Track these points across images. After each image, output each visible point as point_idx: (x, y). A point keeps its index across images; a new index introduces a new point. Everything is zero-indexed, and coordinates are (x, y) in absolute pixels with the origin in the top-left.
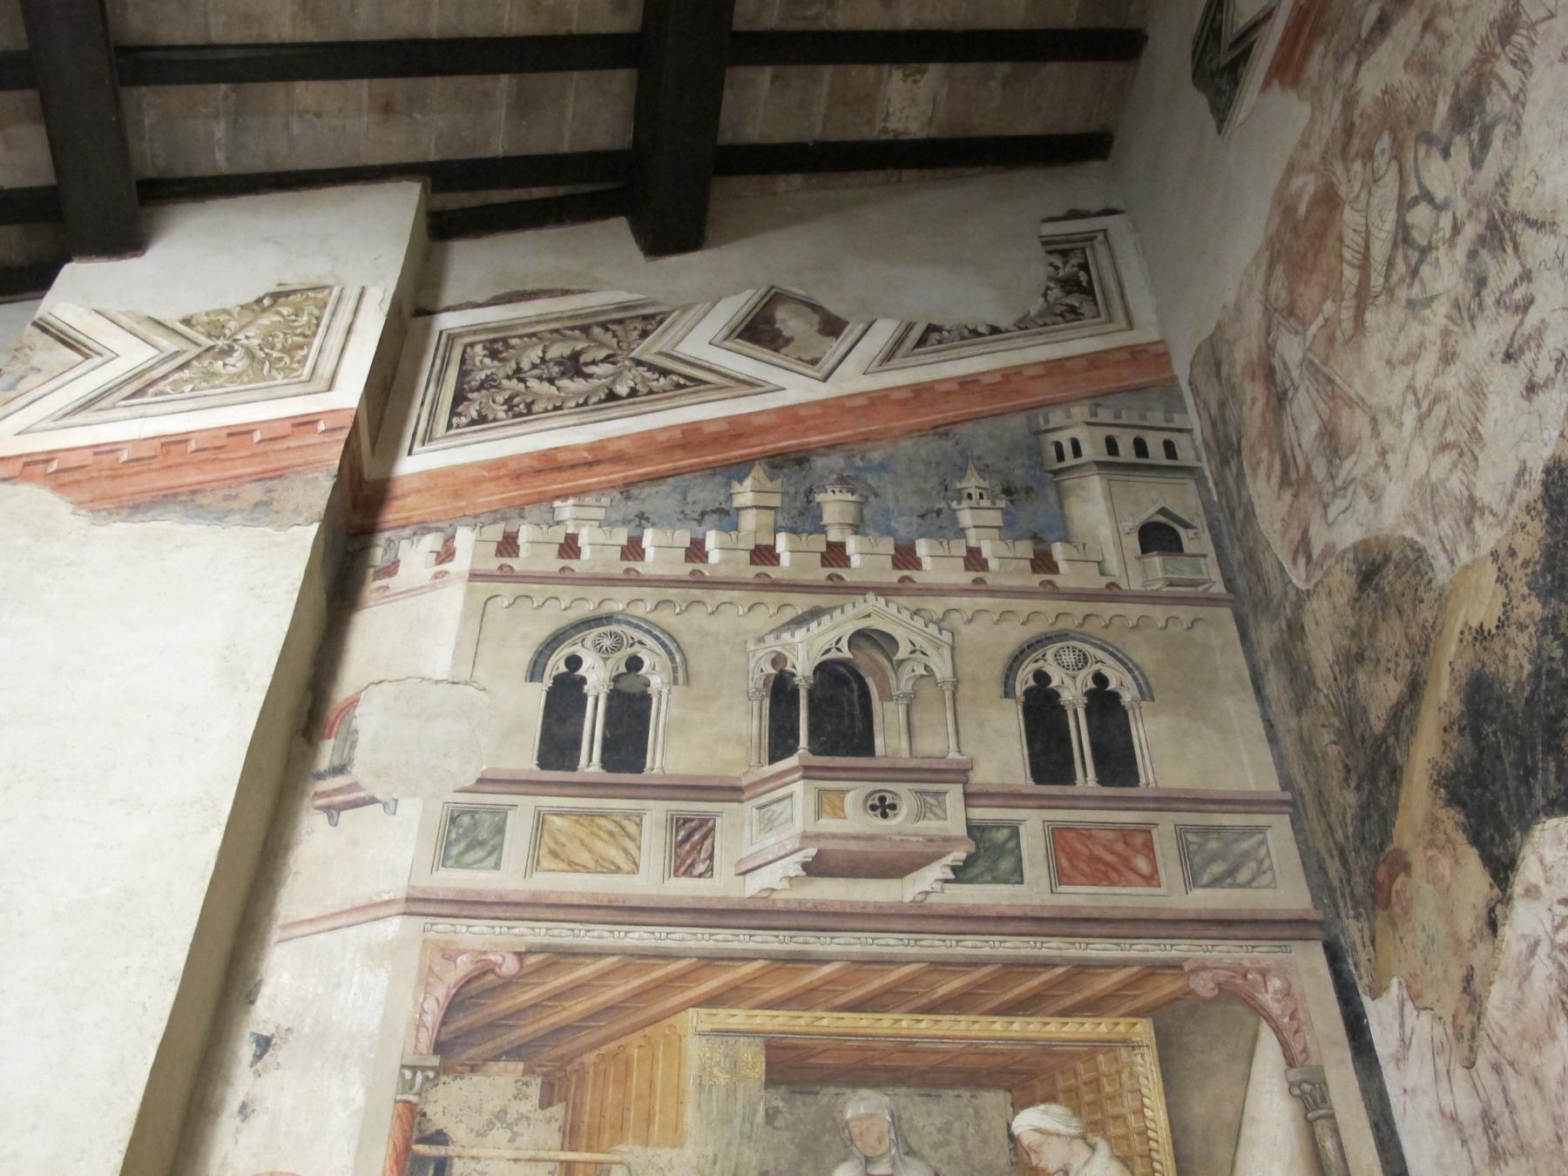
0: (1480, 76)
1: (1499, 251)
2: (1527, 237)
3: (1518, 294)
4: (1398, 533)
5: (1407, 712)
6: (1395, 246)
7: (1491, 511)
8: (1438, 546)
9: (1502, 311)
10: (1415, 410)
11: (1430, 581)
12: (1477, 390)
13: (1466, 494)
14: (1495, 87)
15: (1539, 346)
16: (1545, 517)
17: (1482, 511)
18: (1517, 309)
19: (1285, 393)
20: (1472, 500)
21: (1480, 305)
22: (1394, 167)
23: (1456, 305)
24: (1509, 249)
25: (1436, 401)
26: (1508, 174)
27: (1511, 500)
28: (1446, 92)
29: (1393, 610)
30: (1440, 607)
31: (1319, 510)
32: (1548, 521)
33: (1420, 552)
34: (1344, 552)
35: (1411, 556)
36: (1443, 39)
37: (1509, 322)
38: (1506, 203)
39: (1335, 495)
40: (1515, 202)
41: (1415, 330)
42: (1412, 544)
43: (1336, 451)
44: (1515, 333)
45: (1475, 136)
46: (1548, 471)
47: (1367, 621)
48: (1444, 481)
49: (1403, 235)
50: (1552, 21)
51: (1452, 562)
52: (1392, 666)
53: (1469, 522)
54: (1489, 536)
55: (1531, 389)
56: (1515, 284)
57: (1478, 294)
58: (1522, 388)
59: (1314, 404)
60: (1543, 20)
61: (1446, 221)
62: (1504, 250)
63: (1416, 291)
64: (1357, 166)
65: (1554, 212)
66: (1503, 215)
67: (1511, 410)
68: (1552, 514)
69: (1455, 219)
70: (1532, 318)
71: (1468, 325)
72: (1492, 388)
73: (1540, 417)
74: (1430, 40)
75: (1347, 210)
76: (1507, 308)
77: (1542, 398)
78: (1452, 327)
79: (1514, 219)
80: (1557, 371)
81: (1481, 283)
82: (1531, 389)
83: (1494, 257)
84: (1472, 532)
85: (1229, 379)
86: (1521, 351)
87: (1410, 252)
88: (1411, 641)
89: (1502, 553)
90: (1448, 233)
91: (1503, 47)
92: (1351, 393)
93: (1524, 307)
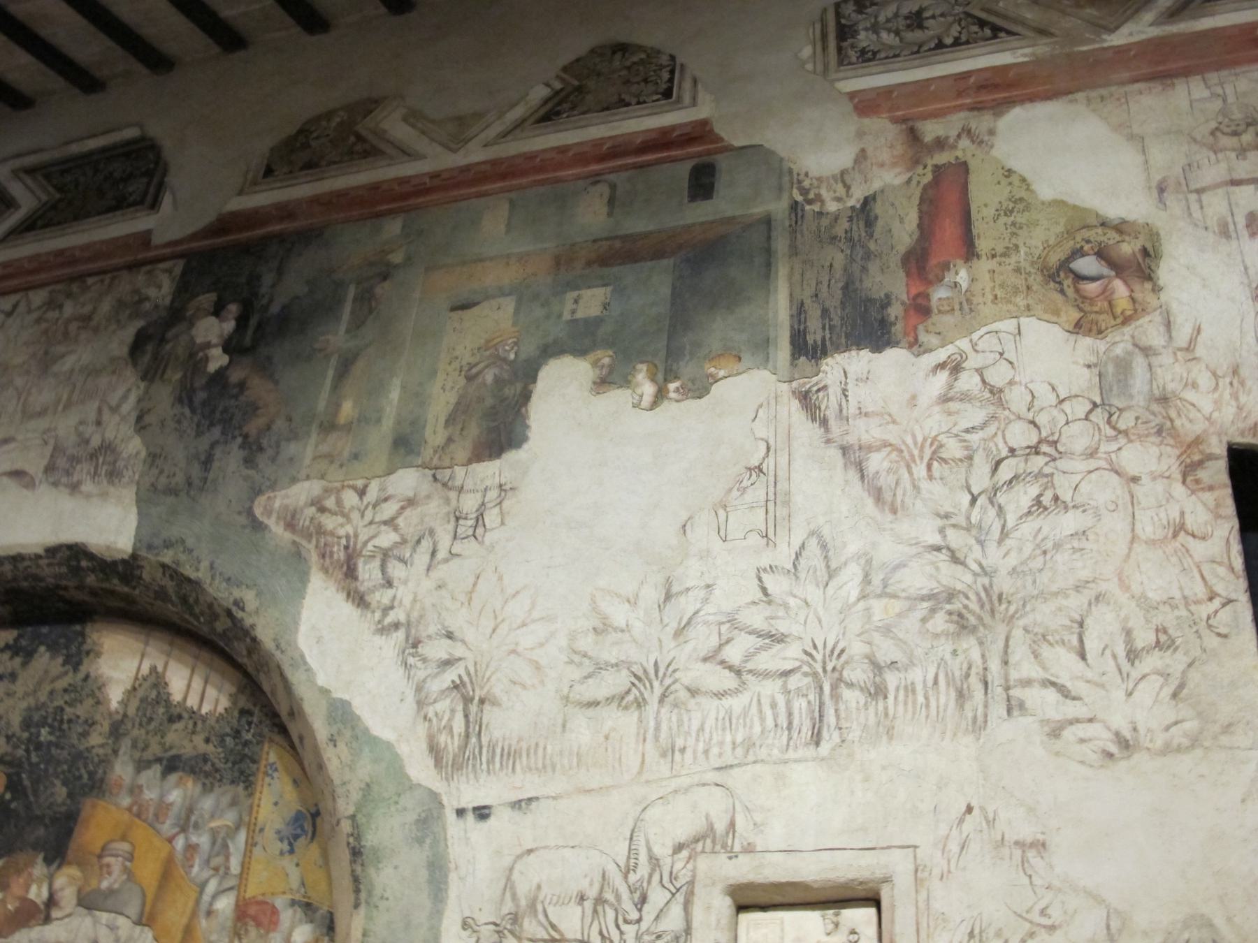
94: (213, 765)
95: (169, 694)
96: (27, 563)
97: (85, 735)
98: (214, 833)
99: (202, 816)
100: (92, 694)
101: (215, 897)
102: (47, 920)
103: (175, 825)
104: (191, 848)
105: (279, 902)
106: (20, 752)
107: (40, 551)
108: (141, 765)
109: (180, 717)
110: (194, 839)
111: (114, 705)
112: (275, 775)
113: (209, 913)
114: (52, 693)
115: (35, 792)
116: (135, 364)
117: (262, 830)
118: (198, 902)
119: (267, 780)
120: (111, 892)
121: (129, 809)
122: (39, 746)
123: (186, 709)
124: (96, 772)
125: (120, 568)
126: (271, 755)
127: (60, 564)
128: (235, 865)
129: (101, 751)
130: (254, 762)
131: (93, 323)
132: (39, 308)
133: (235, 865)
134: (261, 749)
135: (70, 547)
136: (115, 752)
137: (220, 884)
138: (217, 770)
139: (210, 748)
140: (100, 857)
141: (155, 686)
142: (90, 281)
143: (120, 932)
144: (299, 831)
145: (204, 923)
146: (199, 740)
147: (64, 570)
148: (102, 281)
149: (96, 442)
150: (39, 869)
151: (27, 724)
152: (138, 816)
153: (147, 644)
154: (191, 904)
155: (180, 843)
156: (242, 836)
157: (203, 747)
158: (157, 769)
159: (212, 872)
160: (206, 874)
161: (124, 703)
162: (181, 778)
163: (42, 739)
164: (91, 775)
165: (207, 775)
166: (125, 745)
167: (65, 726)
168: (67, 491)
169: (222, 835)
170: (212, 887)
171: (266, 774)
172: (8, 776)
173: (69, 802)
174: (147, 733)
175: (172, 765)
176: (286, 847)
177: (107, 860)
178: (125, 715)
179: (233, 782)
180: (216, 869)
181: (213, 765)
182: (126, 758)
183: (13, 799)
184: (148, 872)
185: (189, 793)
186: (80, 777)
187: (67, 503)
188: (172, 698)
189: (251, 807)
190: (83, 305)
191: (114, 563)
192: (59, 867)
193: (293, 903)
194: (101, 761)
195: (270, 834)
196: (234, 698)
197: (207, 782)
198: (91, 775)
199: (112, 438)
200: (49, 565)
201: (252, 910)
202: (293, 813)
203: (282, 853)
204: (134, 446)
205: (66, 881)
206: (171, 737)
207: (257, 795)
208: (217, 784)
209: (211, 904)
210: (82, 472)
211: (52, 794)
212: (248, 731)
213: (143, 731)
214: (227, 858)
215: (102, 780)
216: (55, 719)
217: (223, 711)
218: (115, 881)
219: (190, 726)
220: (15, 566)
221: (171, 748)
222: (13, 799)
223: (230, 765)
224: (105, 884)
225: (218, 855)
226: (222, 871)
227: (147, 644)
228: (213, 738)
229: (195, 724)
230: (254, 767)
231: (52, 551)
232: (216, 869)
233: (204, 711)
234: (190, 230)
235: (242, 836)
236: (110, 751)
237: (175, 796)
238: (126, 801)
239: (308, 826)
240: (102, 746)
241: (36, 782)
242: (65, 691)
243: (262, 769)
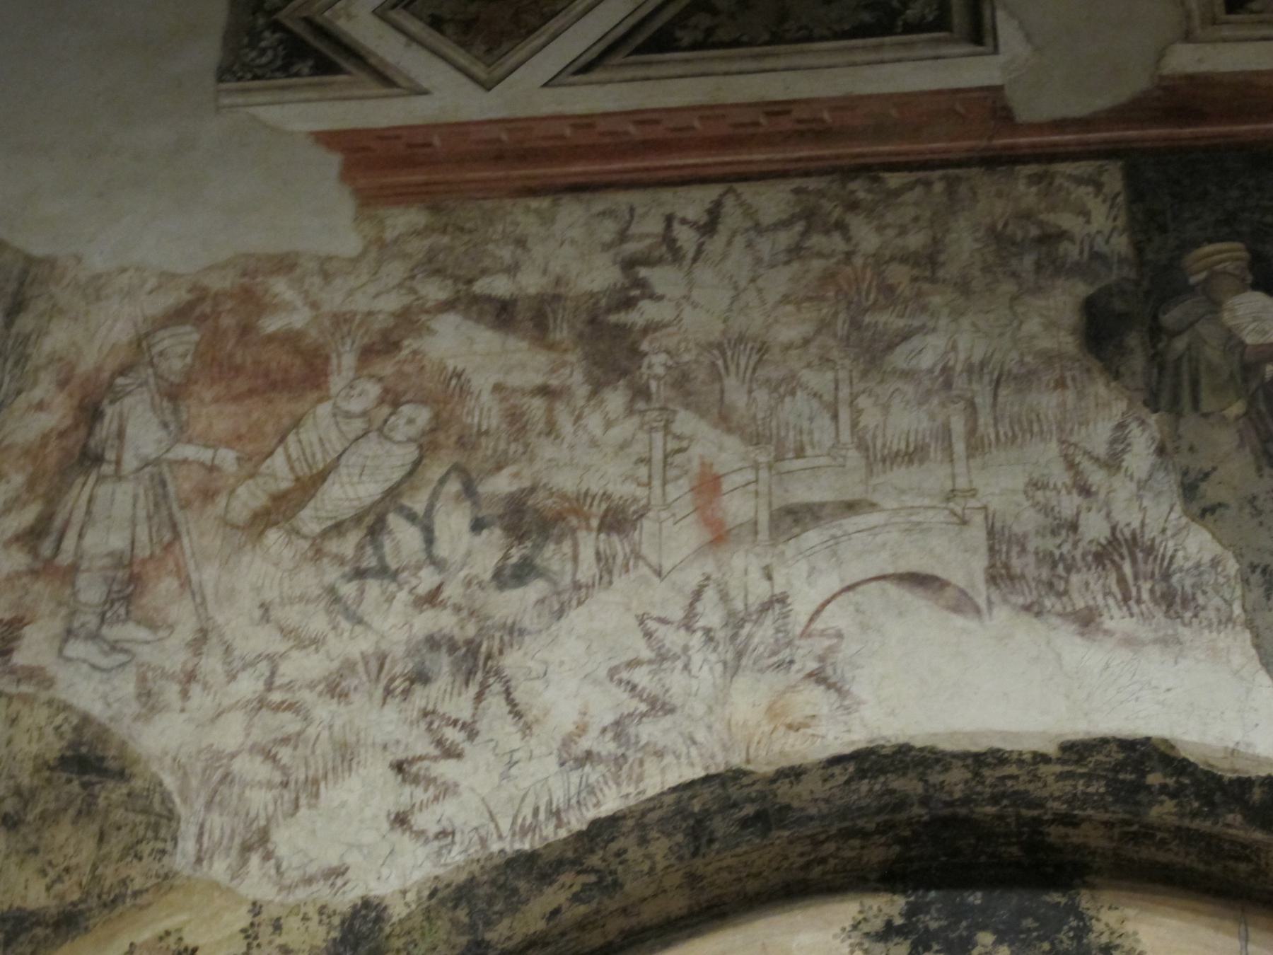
0: (560, 517)
1: (460, 679)
2: (495, 703)
3: (452, 735)
4: (154, 768)
5: (39, 932)
6: (358, 519)
7: (278, 867)
8: (194, 830)
9: (423, 725)
10: (260, 686)
11: (163, 852)
12: (346, 755)
13: (262, 823)
14: (567, 547)
15: (436, 798)
16: (335, 934)
17: (267, 856)
18: (439, 743)
19: (99, 460)
20: (264, 836)
21: (406, 693)
22: (411, 453)
23: (382, 659)
24: (473, 689)
25: (291, 707)
26: (522, 632)
27: (309, 881)
28: (516, 475)
29: (94, 828)
30: (158, 886)
31: (57, 626)
32: (334, 940)
33: (171, 816)
34: (66, 707)
35: (157, 806)
36: (551, 429)
37: (422, 746)
38: (501, 652)
39: (94, 636)
40: (511, 661)
41: (318, 623)
42: (166, 798)
43: (128, 600)
44: (421, 758)
45: (516, 555)
46: (366, 903)
47: (47, 800)
48: (245, 785)
49: (373, 523)
50: (656, 580)
51: (199, 860)
52: (52, 874)
53: (246, 849)
54: (257, 883)
55: (401, 820)
56: (455, 723)
57: (412, 682)
58: (394, 810)
59: (133, 523)
60: (650, 566)
61: (427, 580)
62: (467, 684)
63: (348, 590)
64: (374, 390)
65: (537, 721)
66: (489, 657)
67: (368, 813)
68: (343, 940)
69: (439, 589)
70: (446, 769)
71: (379, 693)
72: (362, 771)
73: (392, 852)
74: (537, 406)
75: (324, 409)
76: (429, 729)
77: (404, 841)
78: (360, 668)
79: (498, 673)
80: (437, 836)
81: (421, 677)
82: (401, 820)
83: (453, 675)
84: (244, 862)
85: (25, 340)
86: (416, 780)
87: (369, 550)
88: (95, 878)
89: (264, 916)
90: (423, 589)
91: (600, 530)
92: (194, 577)
93: (451, 753)
96: (1013, 770)
107: (1051, 749)
116: (1115, 375)
125: (1257, 794)
127: (1089, 777)
131: (950, 271)
132: (786, 224)
135: (1128, 745)
142: (894, 180)
147: (1098, 787)
148: (928, 184)
149: (1095, 528)
153: (1247, 939)
168: (1073, 627)
187: (1076, 651)
190: (903, 231)
191: (1244, 784)
199: (1136, 524)
200: (1061, 777)
204: (1198, 544)
210: (1088, 587)
220: (976, 774)
227: (1247, 939)
231: (1077, 751)
234: (1102, 102)
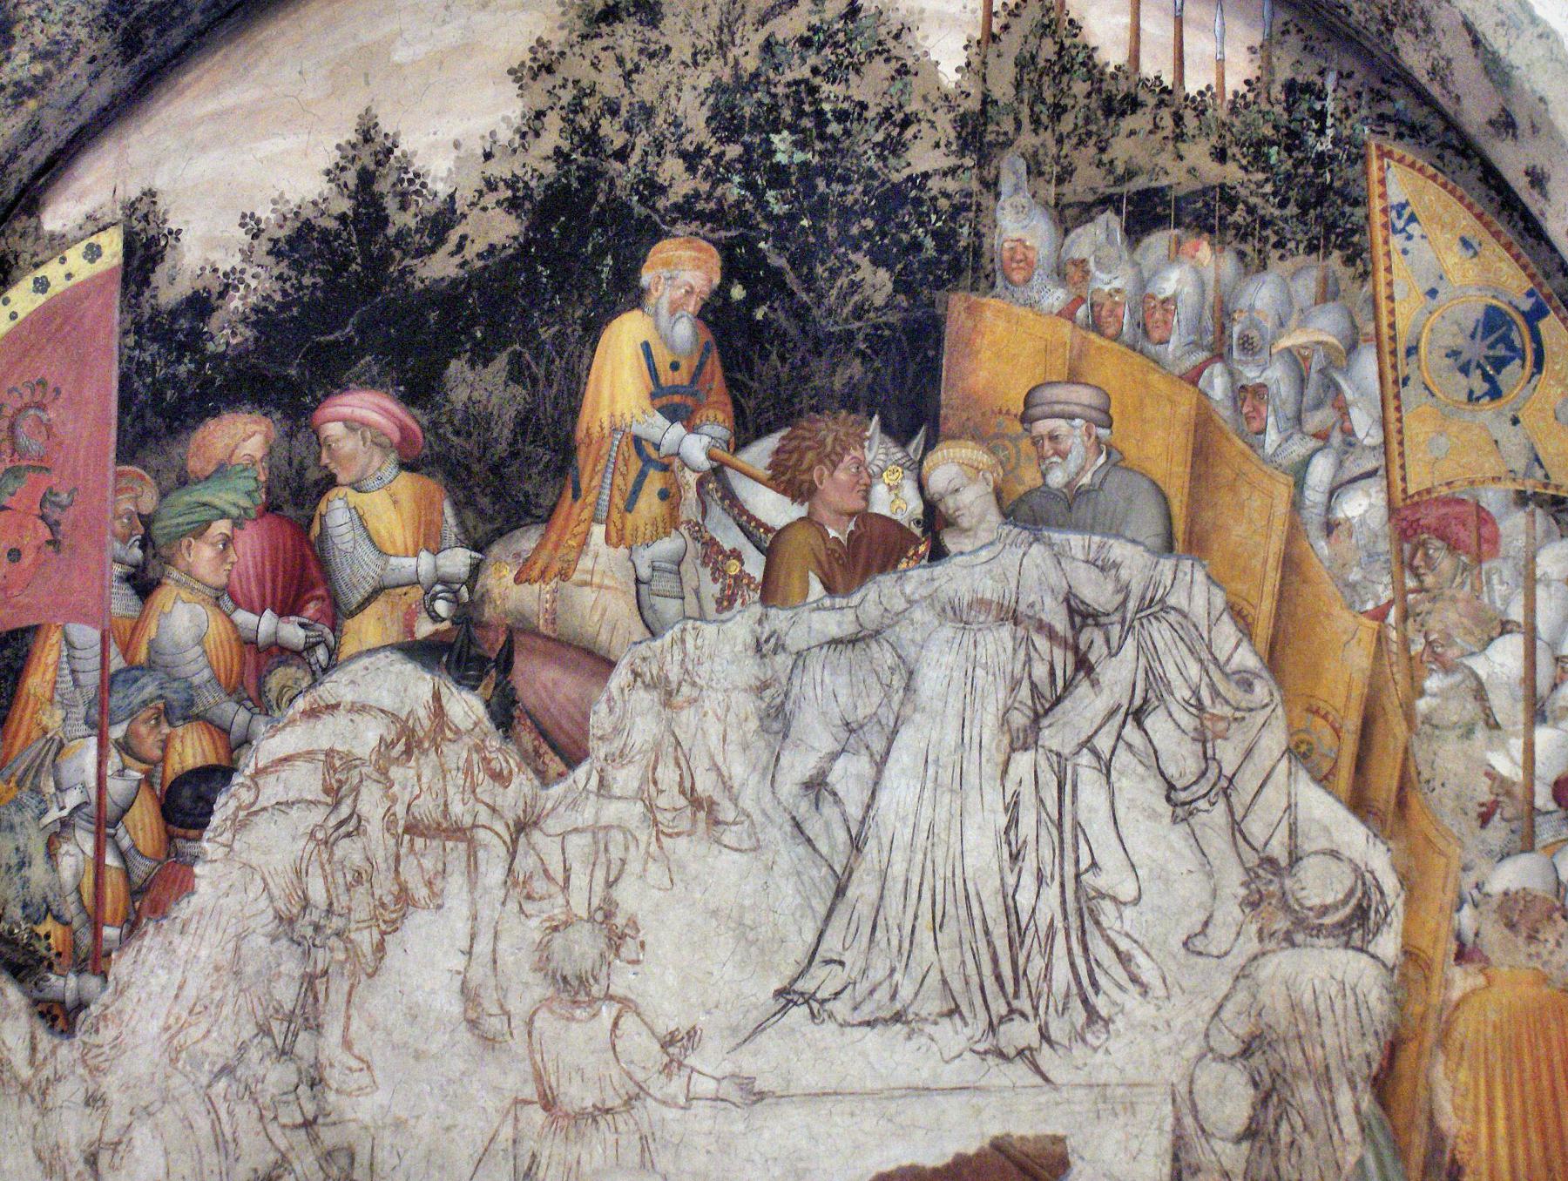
94: (1251, 210)
95: (1090, 51)
97: (893, 148)
98: (1297, 361)
99: (1255, 324)
100: (881, 50)
101: (1335, 491)
102: (938, 554)
103: (1196, 345)
104: (1247, 395)
105: (1493, 498)
106: (733, 191)
108: (1069, 216)
109: (1133, 104)
110: (1251, 374)
111: (949, 76)
112: (1413, 228)
113: (1330, 527)
114: (768, 46)
115: (809, 281)
117: (1412, 351)
118: (1296, 505)
119: (1397, 242)
120: (1074, 496)
121: (1068, 313)
122: (779, 177)
123: (1143, 82)
124: (954, 233)
126: (1398, 180)
128: (1364, 423)
129: (951, 185)
130: (1356, 203)
133: (1364, 423)
134: (1366, 172)
136: (991, 185)
137: (1340, 464)
138: (1265, 223)
139: (1232, 173)
140: (1026, 419)
141: (1047, 28)
143: (1124, 574)
144: (1501, 351)
145: (1323, 547)
146: (1198, 153)
150: (877, 449)
151: (726, 123)
152: (1096, 326)
154: (1282, 508)
155: (1217, 383)
156: (1367, 364)
157: (1213, 172)
158: (1108, 225)
159: (1313, 444)
160: (1298, 448)
161: (976, 68)
162: (1179, 243)
163: (781, 158)
164: (944, 239)
165: (1243, 234)
166: (1011, 169)
167: (834, 128)
169: (1316, 363)
170: (1321, 471)
171: (1389, 227)
172: (726, 249)
173: (902, 299)
174: (1060, 141)
175: (1145, 213)
176: (1481, 387)
177: (1043, 426)
178: (986, 100)
179: (1312, 248)
180: (1323, 436)
181: (1251, 210)
182: (1023, 199)
183: (752, 300)
184: (1161, 448)
185: (1210, 276)
186: (916, 246)
188: (1099, 58)
189: (1374, 301)
192: (929, 446)
193: (1522, 499)
194: (958, 210)
195: (1432, 359)
196: (1264, 52)
197: (1247, 248)
198: (944, 239)
201: (1430, 517)
202: (1478, 313)
203: (1472, 398)
205: (955, 470)
206: (1122, 150)
207: (1382, 276)
208: (1275, 254)
209: (1329, 509)
211: (855, 286)
212: (1321, 132)
213: (1047, 137)
214: (1343, 410)
215: (977, 253)
216: (799, 113)
217: (1243, 89)
218: (1081, 470)
219: (1167, 122)
221: (1130, 174)
222: (752, 300)
223: (1292, 210)
224: (1057, 478)
225: (1318, 406)
226: (1336, 438)
228: (1233, 150)
229: (1178, 119)
230: (1359, 212)
232: (1323, 436)
233: (1192, 87)
235: (1367, 364)
236: (975, 186)
237: (1174, 281)
238: (1056, 297)
239: (1520, 336)
240: (952, 172)
241: (802, 259)
242: (805, 43)
243: (1378, 218)
